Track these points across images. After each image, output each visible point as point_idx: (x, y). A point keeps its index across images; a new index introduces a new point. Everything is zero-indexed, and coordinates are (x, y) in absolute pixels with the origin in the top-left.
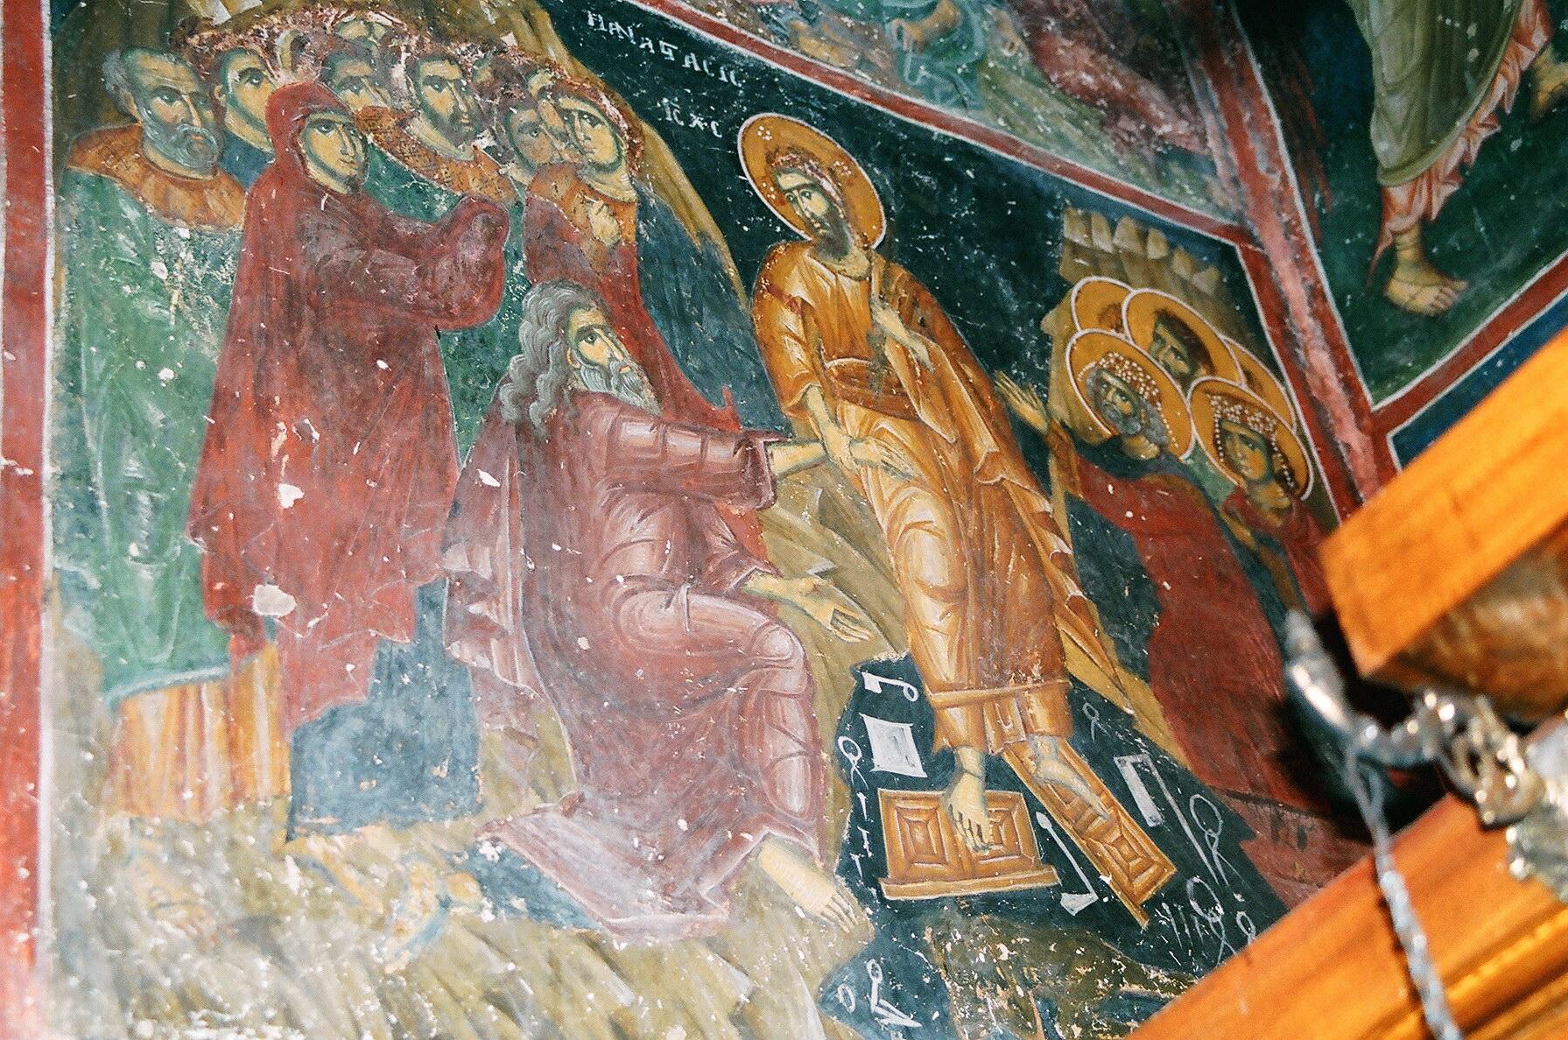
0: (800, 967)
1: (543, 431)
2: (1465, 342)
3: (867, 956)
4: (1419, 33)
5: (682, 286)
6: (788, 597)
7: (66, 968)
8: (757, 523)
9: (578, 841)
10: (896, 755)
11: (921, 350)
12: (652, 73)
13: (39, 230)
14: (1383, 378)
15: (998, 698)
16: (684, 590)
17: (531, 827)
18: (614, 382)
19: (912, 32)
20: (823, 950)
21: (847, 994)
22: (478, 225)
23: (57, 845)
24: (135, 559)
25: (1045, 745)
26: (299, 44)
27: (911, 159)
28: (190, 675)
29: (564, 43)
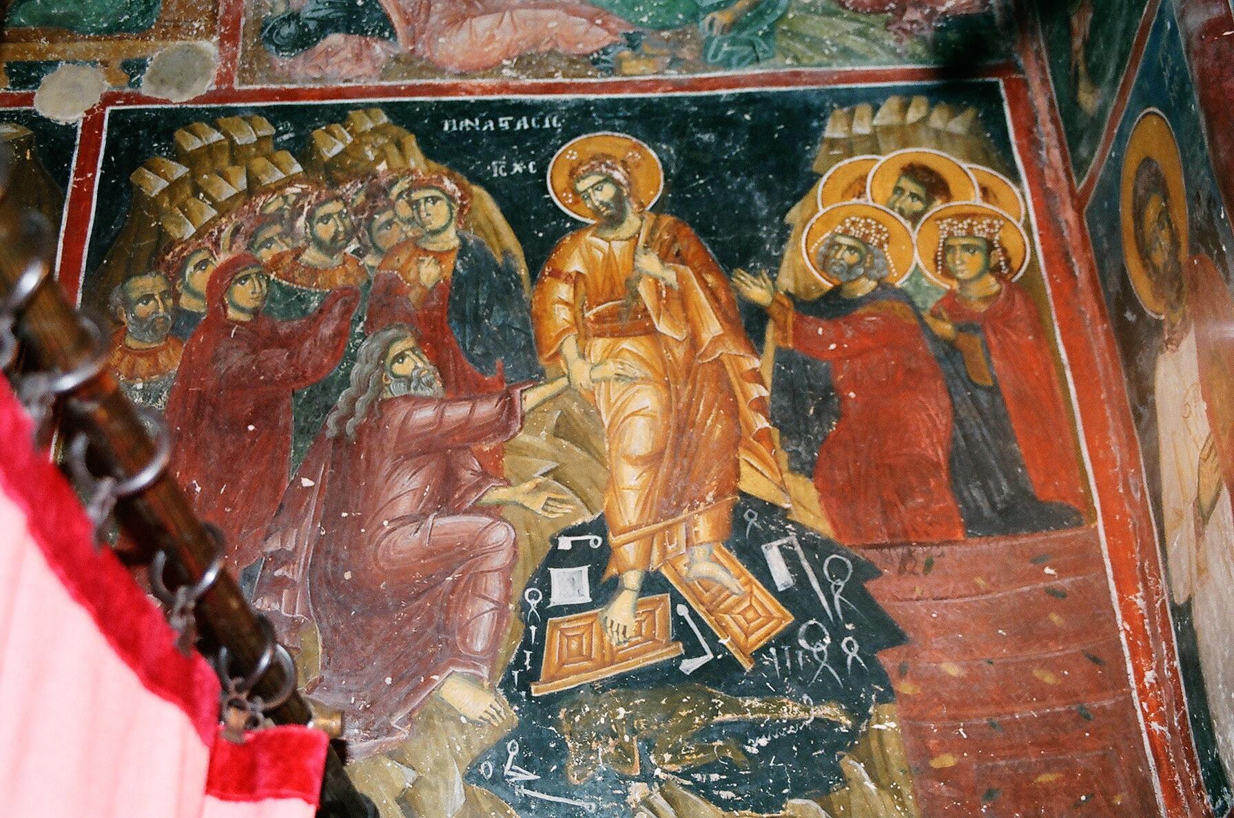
5: (480, 297)
8: (499, 452)
10: (570, 589)
12: (489, 145)
15: (669, 527)
16: (431, 518)
19: (722, 18)
20: (475, 742)
22: (337, 310)
26: (236, 230)
27: (695, 126)
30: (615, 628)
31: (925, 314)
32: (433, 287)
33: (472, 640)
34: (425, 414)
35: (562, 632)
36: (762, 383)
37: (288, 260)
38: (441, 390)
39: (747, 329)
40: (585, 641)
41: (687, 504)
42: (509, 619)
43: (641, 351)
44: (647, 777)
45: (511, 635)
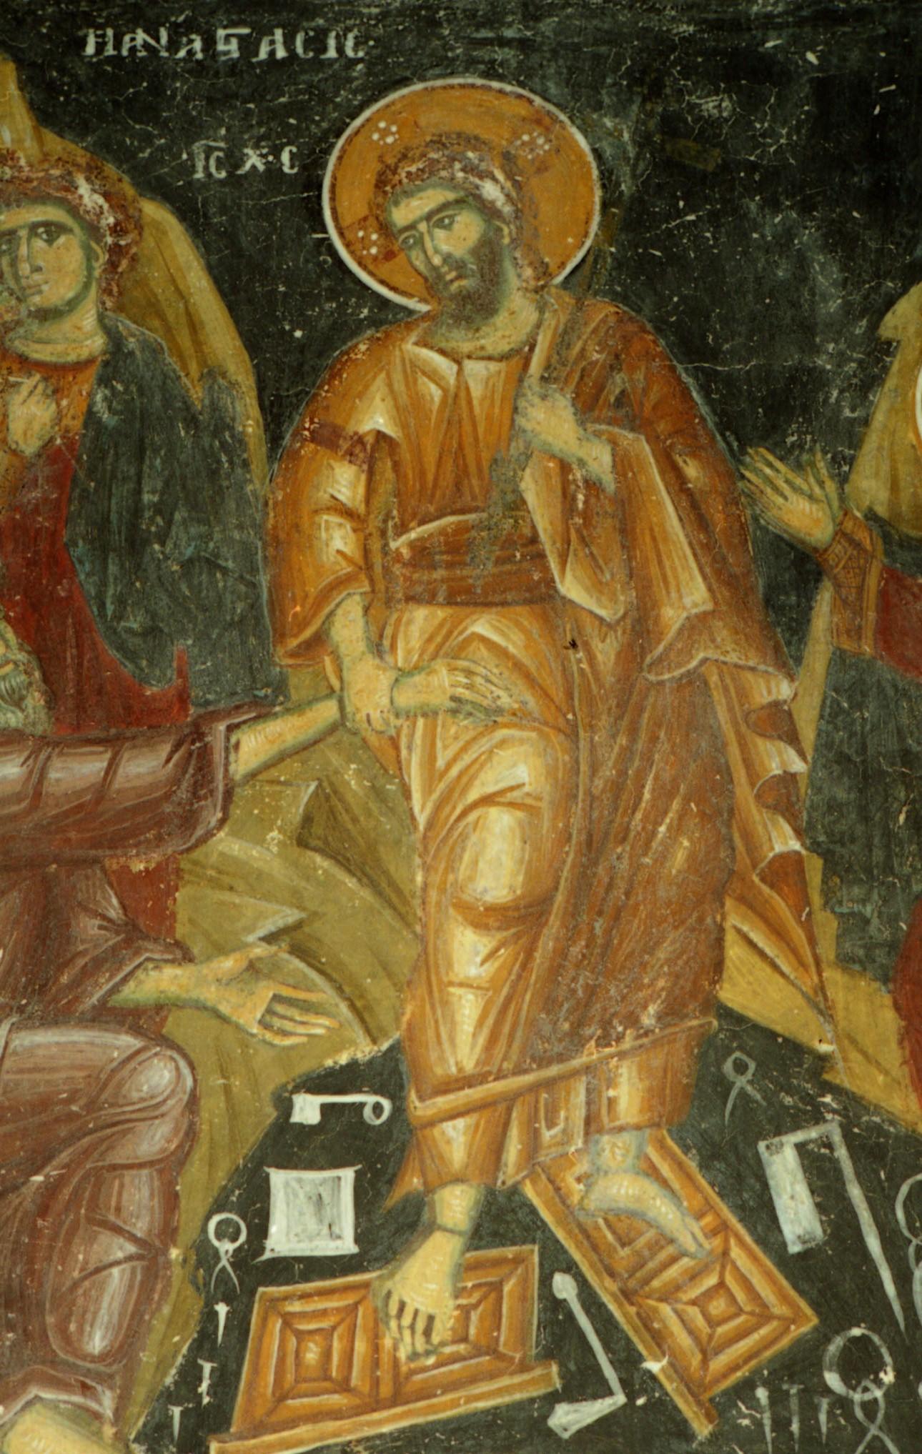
6: (195, 994)
10: (312, 1224)
12: (187, 99)
15: (549, 1084)
25: (615, 1151)
29: (32, 106)
30: (406, 1321)
32: (39, 455)
33: (81, 1329)
35: (288, 1320)
36: (792, 738)
38: (43, 715)
39: (768, 602)
40: (336, 1345)
41: (593, 1030)
42: (169, 1284)
43: (514, 643)
45: (170, 1322)
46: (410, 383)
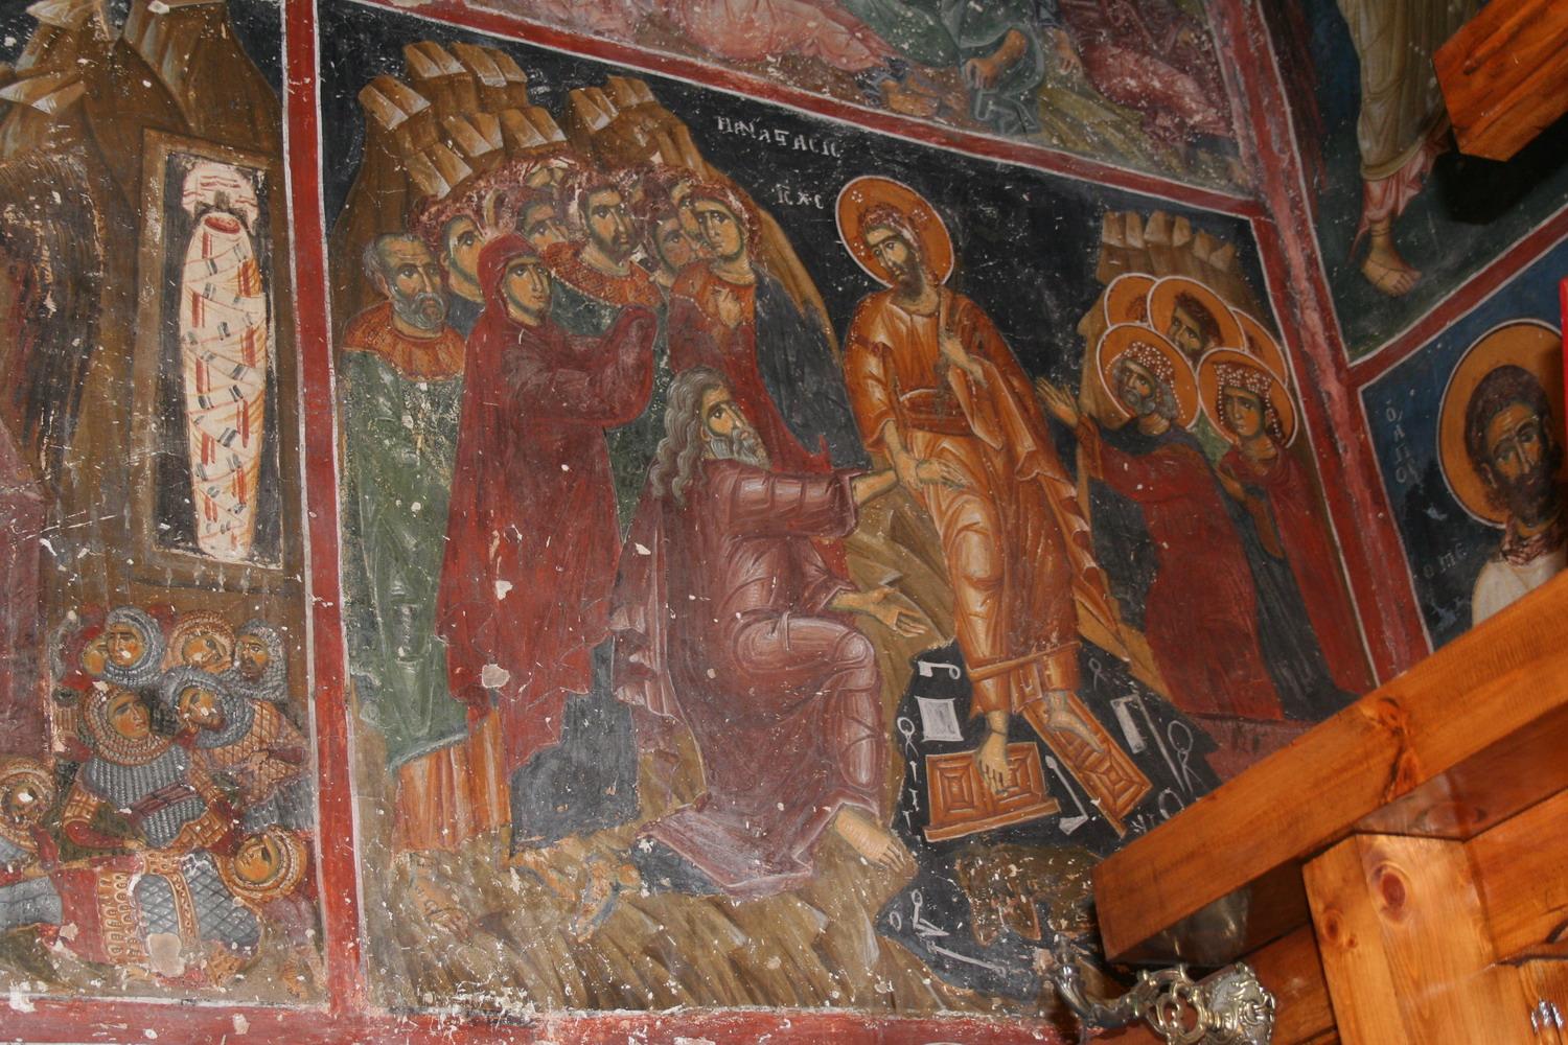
0: (863, 902)
1: (683, 500)
2: (1416, 322)
3: (910, 888)
4: (1395, 55)
5: (789, 353)
6: (865, 608)
7: (378, 962)
8: (840, 549)
9: (706, 829)
10: (941, 726)
11: (977, 371)
12: (768, 162)
13: (326, 408)
14: (1358, 341)
15: (1022, 666)
16: (785, 617)
17: (674, 824)
18: (735, 448)
19: (983, 68)
20: (879, 887)
21: (895, 918)
22: (634, 332)
23: (366, 879)
24: (403, 659)
25: (1056, 699)
26: (499, 201)
27: (977, 193)
28: (442, 743)
29: (701, 151)
31: (1216, 466)
34: (754, 487)
37: (567, 254)
38: (766, 461)
43: (961, 453)
44: (1047, 944)
46: (892, 322)
